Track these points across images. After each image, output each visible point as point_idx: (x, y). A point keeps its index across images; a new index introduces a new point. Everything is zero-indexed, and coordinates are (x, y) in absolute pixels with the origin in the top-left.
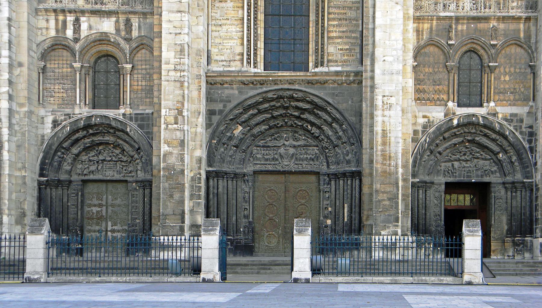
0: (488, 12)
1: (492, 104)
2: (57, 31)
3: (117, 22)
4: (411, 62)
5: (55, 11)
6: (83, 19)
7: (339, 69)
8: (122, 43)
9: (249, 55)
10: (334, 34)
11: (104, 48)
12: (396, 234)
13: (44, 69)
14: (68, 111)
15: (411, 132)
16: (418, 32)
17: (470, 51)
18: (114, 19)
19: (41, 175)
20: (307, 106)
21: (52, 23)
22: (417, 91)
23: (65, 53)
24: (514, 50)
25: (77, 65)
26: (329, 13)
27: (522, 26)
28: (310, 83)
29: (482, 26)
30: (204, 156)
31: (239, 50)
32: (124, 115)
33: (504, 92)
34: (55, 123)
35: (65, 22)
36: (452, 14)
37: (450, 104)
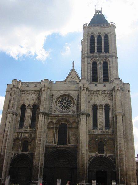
0: (104, 133)
1: (106, 153)
2: (17, 136)
3: (29, 134)
4: (88, 144)
5: (17, 132)
6: (23, 134)
7: (73, 145)
8: (29, 138)
9: (54, 142)
10: (72, 137)
11: (26, 139)
12: (84, 183)
13: (14, 144)
14: (17, 152)
15: (88, 159)
16: (90, 137)
17: (100, 141)
18: (28, 134)
19: (11, 166)
20: (66, 153)
21: (17, 134)
22: (90, 150)
23: (18, 140)
24: (110, 141)
25: (20, 143)
26: (71, 133)
27: (111, 136)
28: (67, 148)
29: (103, 136)
30: (43, 163)
31: (52, 140)
32: (28, 153)
33: (108, 150)
34: (15, 155)
35: (19, 134)
36: (97, 134)
37: (97, 153)
